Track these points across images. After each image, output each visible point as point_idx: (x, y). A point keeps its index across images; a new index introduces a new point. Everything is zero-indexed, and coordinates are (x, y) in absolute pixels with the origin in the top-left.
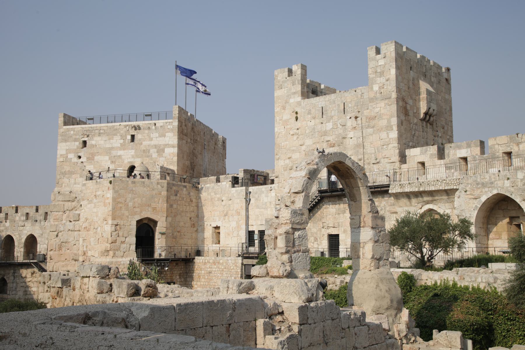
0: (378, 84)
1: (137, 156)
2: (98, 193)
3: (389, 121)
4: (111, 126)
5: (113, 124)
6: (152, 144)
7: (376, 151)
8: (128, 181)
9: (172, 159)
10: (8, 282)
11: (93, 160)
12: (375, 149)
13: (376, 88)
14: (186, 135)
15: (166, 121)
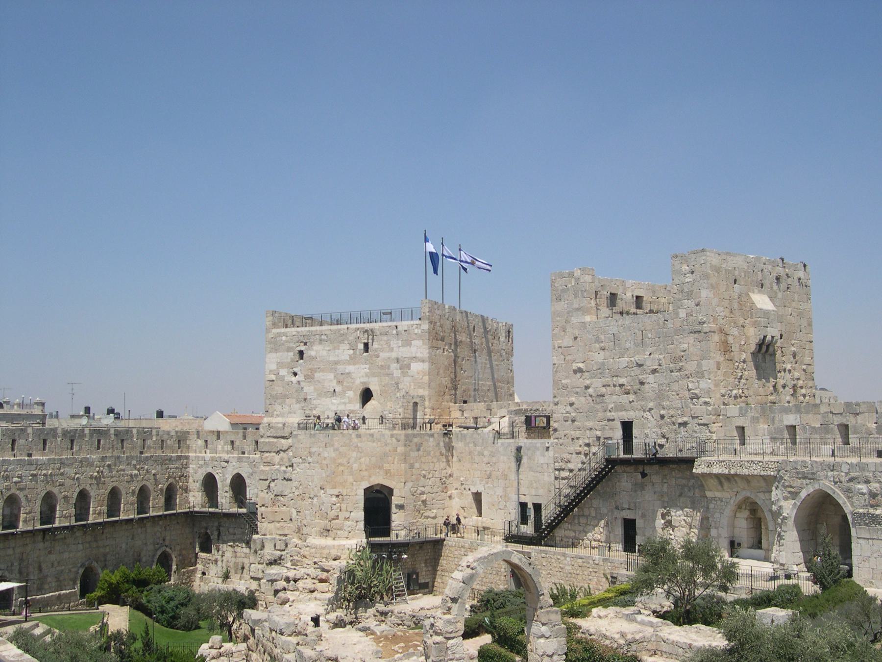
0: (685, 309)
1: (374, 375)
2: (313, 450)
3: (699, 365)
4: (337, 330)
5: (339, 327)
6: (393, 357)
7: (683, 404)
8: (351, 435)
9: (422, 379)
10: (212, 537)
11: (313, 378)
12: (681, 402)
13: (682, 314)
14: (443, 339)
15: (412, 322)
